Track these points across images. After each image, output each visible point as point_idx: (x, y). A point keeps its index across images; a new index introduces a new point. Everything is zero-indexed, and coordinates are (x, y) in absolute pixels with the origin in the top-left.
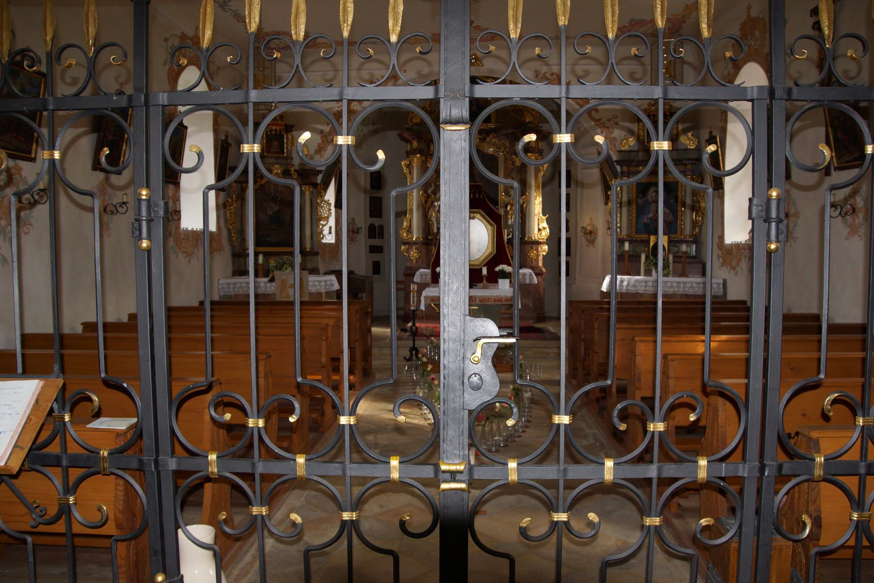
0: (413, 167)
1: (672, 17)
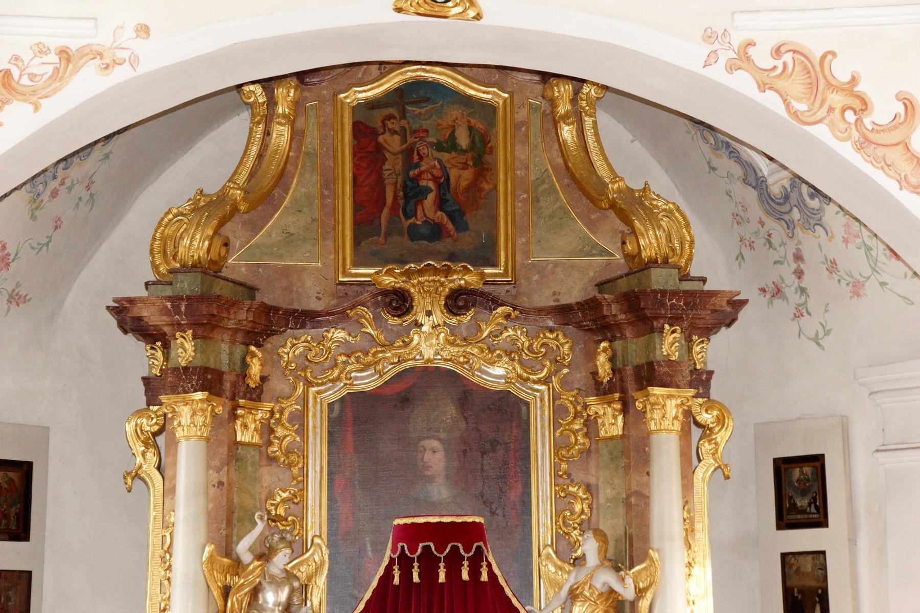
0: (173, 443)
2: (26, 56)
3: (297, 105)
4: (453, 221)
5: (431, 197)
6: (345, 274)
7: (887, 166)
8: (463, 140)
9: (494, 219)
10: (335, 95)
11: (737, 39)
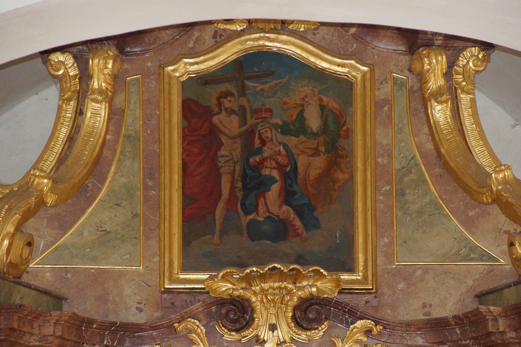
4: (302, 218)
5: (275, 188)
6: (172, 281)
9: (351, 215)
10: (162, 67)
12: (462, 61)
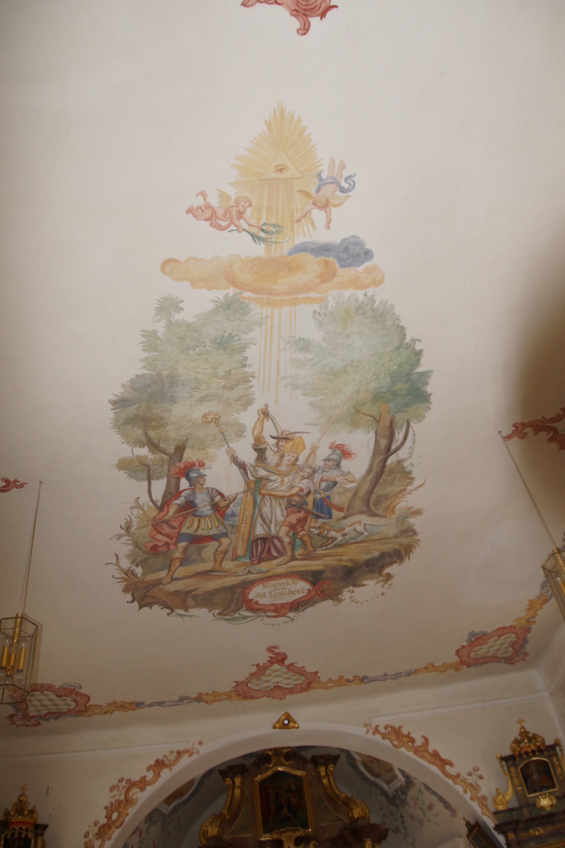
1: (515, 623)
2: (168, 755)
3: (242, 783)
5: (285, 809)
7: (423, 757)
8: (293, 788)
11: (374, 725)
12: (329, 768)
